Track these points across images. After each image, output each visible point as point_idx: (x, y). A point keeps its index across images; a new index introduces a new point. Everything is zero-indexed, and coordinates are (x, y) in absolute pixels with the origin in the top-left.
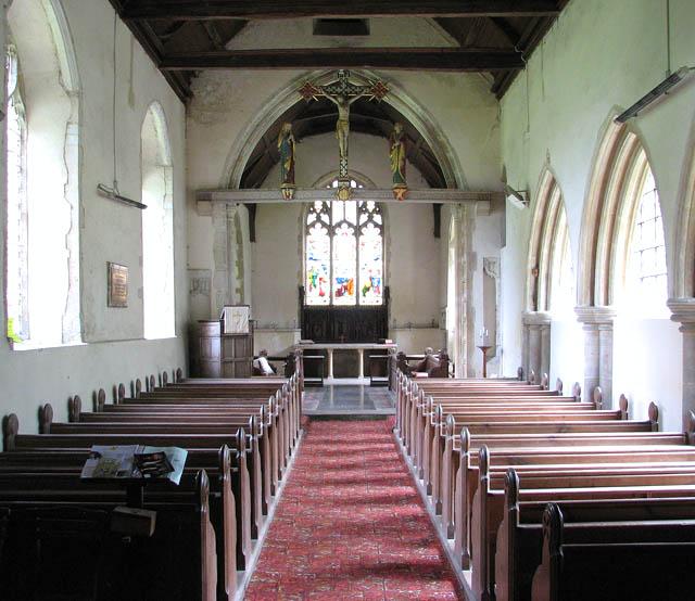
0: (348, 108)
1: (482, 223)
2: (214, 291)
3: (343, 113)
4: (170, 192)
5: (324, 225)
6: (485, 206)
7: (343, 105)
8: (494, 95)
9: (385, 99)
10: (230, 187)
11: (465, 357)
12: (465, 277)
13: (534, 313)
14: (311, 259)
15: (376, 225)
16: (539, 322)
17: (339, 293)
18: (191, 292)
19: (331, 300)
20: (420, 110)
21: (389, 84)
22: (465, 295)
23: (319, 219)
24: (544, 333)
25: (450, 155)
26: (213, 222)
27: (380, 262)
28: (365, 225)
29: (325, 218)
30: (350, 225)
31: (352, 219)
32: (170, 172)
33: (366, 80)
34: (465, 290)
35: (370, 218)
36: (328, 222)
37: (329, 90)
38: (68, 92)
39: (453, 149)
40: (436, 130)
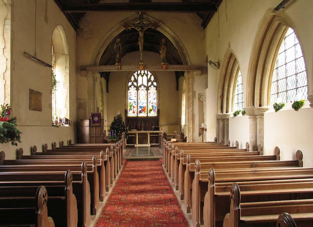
0: (143, 32)
1: (198, 79)
2: (87, 108)
3: (141, 34)
4: (68, 65)
5: (135, 86)
6: (199, 72)
7: (141, 31)
8: (203, 27)
9: (158, 29)
10: (95, 65)
11: (191, 134)
12: (191, 101)
13: (221, 114)
14: (130, 99)
15: (154, 86)
16: (224, 118)
17: (140, 112)
18: (78, 108)
19: (137, 115)
20: (172, 33)
21: (160, 23)
22: (191, 109)
23: (133, 84)
24: (226, 123)
25: (185, 52)
26: (87, 79)
27: (156, 100)
28: (150, 86)
29: (135, 84)
30: (145, 86)
31: (146, 84)
32: (68, 58)
33: (151, 22)
34: (191, 107)
36: (136, 85)
37: (136, 25)
38: (5, 4)
39: (186, 49)
40: (179, 41)
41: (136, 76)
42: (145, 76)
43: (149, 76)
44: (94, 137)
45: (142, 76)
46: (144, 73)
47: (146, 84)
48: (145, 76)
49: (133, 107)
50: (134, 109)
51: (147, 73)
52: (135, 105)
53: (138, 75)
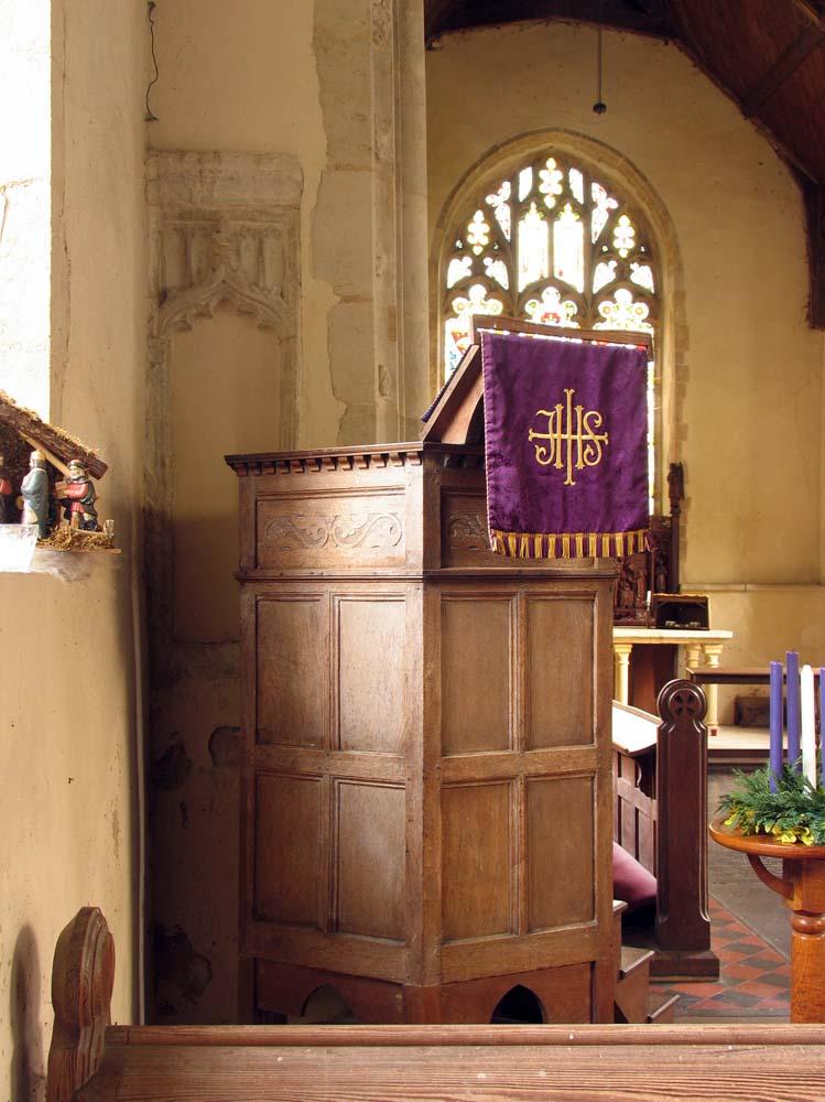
2: (316, 296)
15: (639, 294)
18: (163, 297)
23: (478, 270)
28: (608, 293)
30: (566, 292)
35: (623, 275)
36: (504, 282)
41: (503, 215)
42: (568, 216)
43: (599, 219)
44: (505, 780)
45: (551, 216)
46: (565, 196)
48: (568, 216)
53: (518, 208)
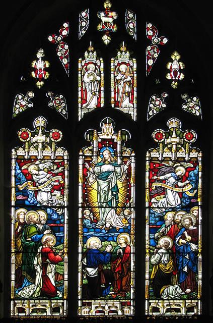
5: (54, 120)
14: (20, 204)
15: (188, 121)
17: (93, 291)
19: (73, 307)
23: (40, 106)
27: (197, 211)
28: (161, 120)
29: (58, 104)
30: (120, 121)
31: (128, 107)
35: (174, 108)
36: (62, 109)
41: (63, 51)
42: (124, 56)
43: (152, 56)
45: (107, 54)
46: (121, 35)
47: (128, 107)
48: (124, 56)
49: (45, 255)
50: (51, 268)
51: (141, 29)
52: (59, 241)
53: (77, 49)
